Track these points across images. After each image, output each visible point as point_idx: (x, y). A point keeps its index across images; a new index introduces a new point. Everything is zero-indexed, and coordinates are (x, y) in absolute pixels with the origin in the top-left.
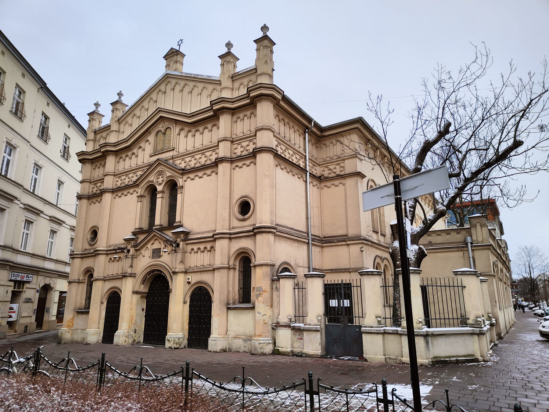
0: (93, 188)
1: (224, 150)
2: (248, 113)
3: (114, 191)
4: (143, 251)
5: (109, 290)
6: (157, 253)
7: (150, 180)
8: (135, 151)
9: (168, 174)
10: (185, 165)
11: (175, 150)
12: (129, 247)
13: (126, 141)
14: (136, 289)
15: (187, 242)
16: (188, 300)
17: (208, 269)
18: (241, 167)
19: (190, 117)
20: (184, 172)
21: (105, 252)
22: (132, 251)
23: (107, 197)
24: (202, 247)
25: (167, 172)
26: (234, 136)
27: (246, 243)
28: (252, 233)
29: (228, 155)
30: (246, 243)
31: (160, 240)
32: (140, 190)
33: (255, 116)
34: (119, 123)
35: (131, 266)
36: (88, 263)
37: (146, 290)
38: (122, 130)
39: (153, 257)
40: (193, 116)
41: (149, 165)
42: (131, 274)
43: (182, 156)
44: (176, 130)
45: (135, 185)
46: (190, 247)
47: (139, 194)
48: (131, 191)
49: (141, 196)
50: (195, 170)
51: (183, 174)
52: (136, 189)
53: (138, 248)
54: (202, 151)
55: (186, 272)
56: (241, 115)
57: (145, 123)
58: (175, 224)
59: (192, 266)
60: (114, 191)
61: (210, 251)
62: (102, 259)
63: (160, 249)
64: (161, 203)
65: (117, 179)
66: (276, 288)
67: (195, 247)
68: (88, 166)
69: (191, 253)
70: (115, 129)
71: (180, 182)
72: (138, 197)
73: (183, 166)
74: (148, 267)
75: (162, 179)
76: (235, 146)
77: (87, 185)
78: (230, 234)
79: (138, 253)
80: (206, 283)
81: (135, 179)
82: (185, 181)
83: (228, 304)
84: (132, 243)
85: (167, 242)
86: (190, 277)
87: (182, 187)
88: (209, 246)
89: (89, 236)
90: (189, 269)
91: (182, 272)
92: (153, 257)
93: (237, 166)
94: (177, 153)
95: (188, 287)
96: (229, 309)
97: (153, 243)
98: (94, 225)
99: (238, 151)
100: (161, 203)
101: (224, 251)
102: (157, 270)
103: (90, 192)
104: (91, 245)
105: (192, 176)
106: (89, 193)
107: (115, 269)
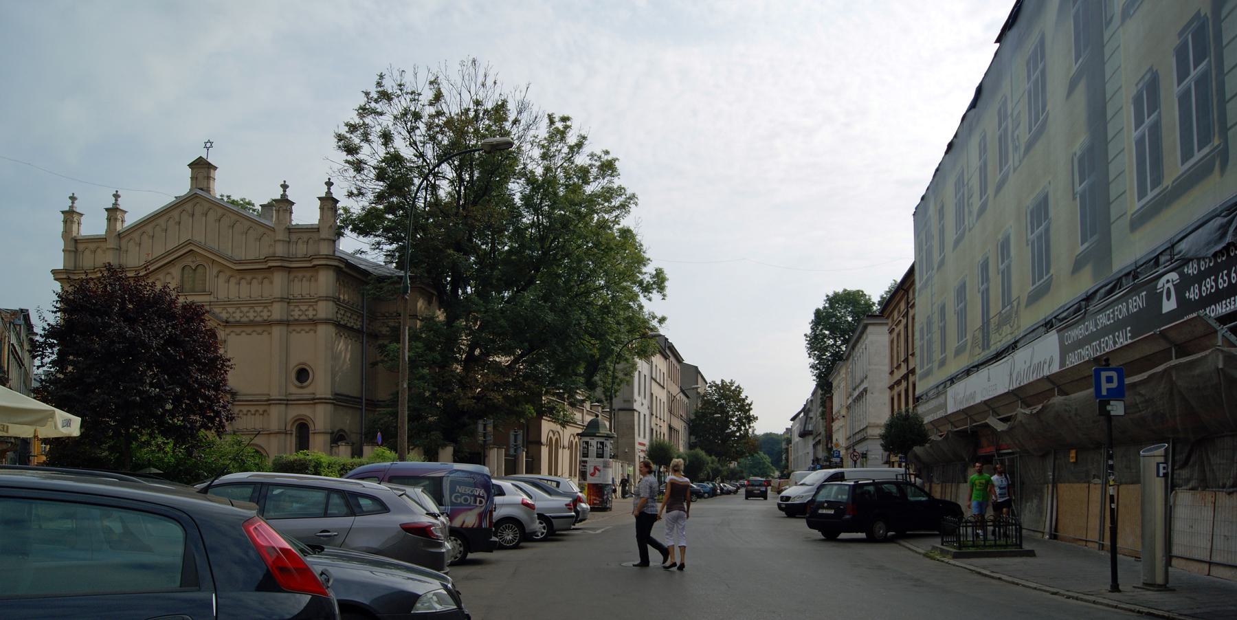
1: (277, 312)
2: (308, 275)
24: (253, 409)
27: (305, 411)
29: (285, 318)
30: (305, 411)
33: (316, 280)
50: (238, 324)
56: (300, 275)
57: (169, 253)
67: (245, 409)
73: (224, 316)
88: (261, 409)
99: (296, 314)
105: (238, 330)
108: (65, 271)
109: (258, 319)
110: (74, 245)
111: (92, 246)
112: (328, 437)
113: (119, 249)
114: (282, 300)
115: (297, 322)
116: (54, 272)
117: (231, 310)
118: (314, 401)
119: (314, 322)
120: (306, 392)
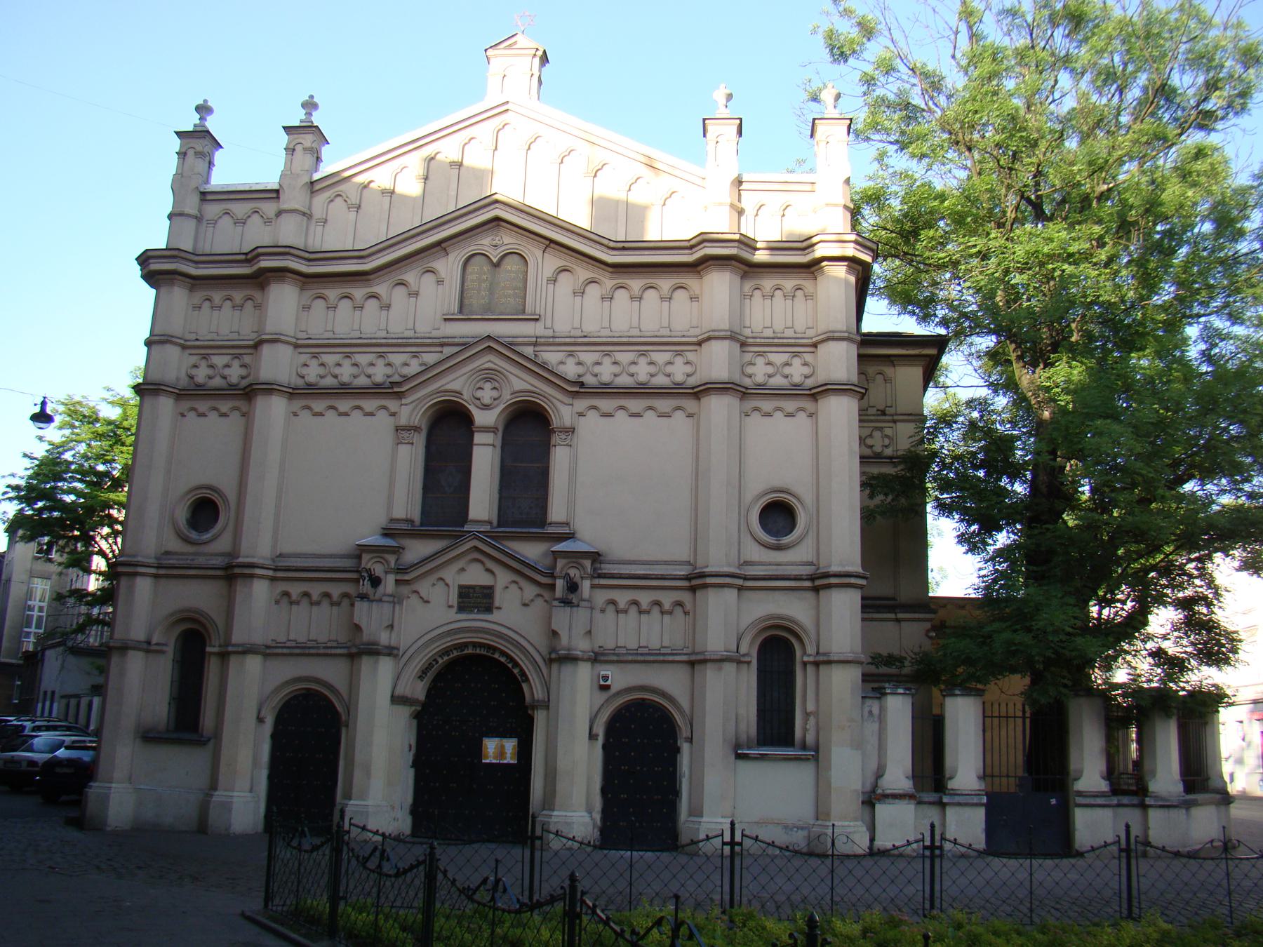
0: (195, 366)
3: (303, 393)
4: (424, 587)
5: (288, 683)
6: (476, 599)
7: (449, 387)
8: (381, 289)
9: (518, 385)
10: (580, 370)
11: (540, 325)
12: (378, 570)
13: (360, 256)
14: (397, 693)
15: (596, 581)
16: (600, 730)
17: (671, 658)
18: (768, 415)
19: (614, 249)
20: (578, 389)
21: (270, 573)
22: (389, 583)
23: (274, 410)
24: (645, 598)
25: (514, 380)
26: (747, 332)
27: (796, 608)
28: (807, 584)
29: (737, 378)
31: (490, 564)
32: (413, 410)
34: (312, 192)
35: (391, 627)
36: (200, 596)
37: (421, 696)
38: (318, 212)
39: (461, 609)
40: (624, 249)
41: (442, 345)
42: (387, 647)
43: (575, 343)
44: (543, 264)
45: (392, 390)
46: (601, 597)
47: (403, 421)
48: (369, 404)
49: (416, 429)
50: (606, 391)
51: (575, 395)
52: (392, 405)
53: (407, 577)
54: (643, 345)
55: (597, 658)
58: (550, 530)
59: (610, 644)
60: (303, 393)
61: (670, 613)
62: (260, 592)
63: (491, 588)
64: (485, 461)
65: (304, 358)
66: (870, 712)
67: (623, 598)
68: (179, 295)
69: (603, 611)
70: (296, 206)
71: (563, 412)
72: (398, 429)
74: (449, 633)
75: (495, 394)
76: (748, 357)
77: (172, 352)
78: (745, 578)
79: (405, 590)
80: (664, 694)
81: (380, 373)
82: (581, 415)
83: (737, 746)
84: (392, 559)
85: (522, 570)
86: (609, 673)
87: (571, 430)
89: (182, 514)
90: (603, 654)
91: (588, 660)
92: (461, 609)
93: (756, 409)
94: (549, 333)
95: (601, 697)
96: (739, 757)
97: (463, 570)
98: (214, 483)
99: (760, 372)
100: (485, 461)
101: (726, 620)
102: (475, 645)
103: (183, 375)
104: (187, 540)
105: (606, 404)
106: (178, 379)
107: (317, 623)
108: (171, 253)
109: (660, 380)
110: (197, 198)
111: (240, 209)
112: (854, 674)
113: (307, 215)
114: (732, 337)
115: (763, 391)
116: (145, 259)
117: (588, 358)
118: (819, 582)
119: (817, 393)
120: (797, 556)
